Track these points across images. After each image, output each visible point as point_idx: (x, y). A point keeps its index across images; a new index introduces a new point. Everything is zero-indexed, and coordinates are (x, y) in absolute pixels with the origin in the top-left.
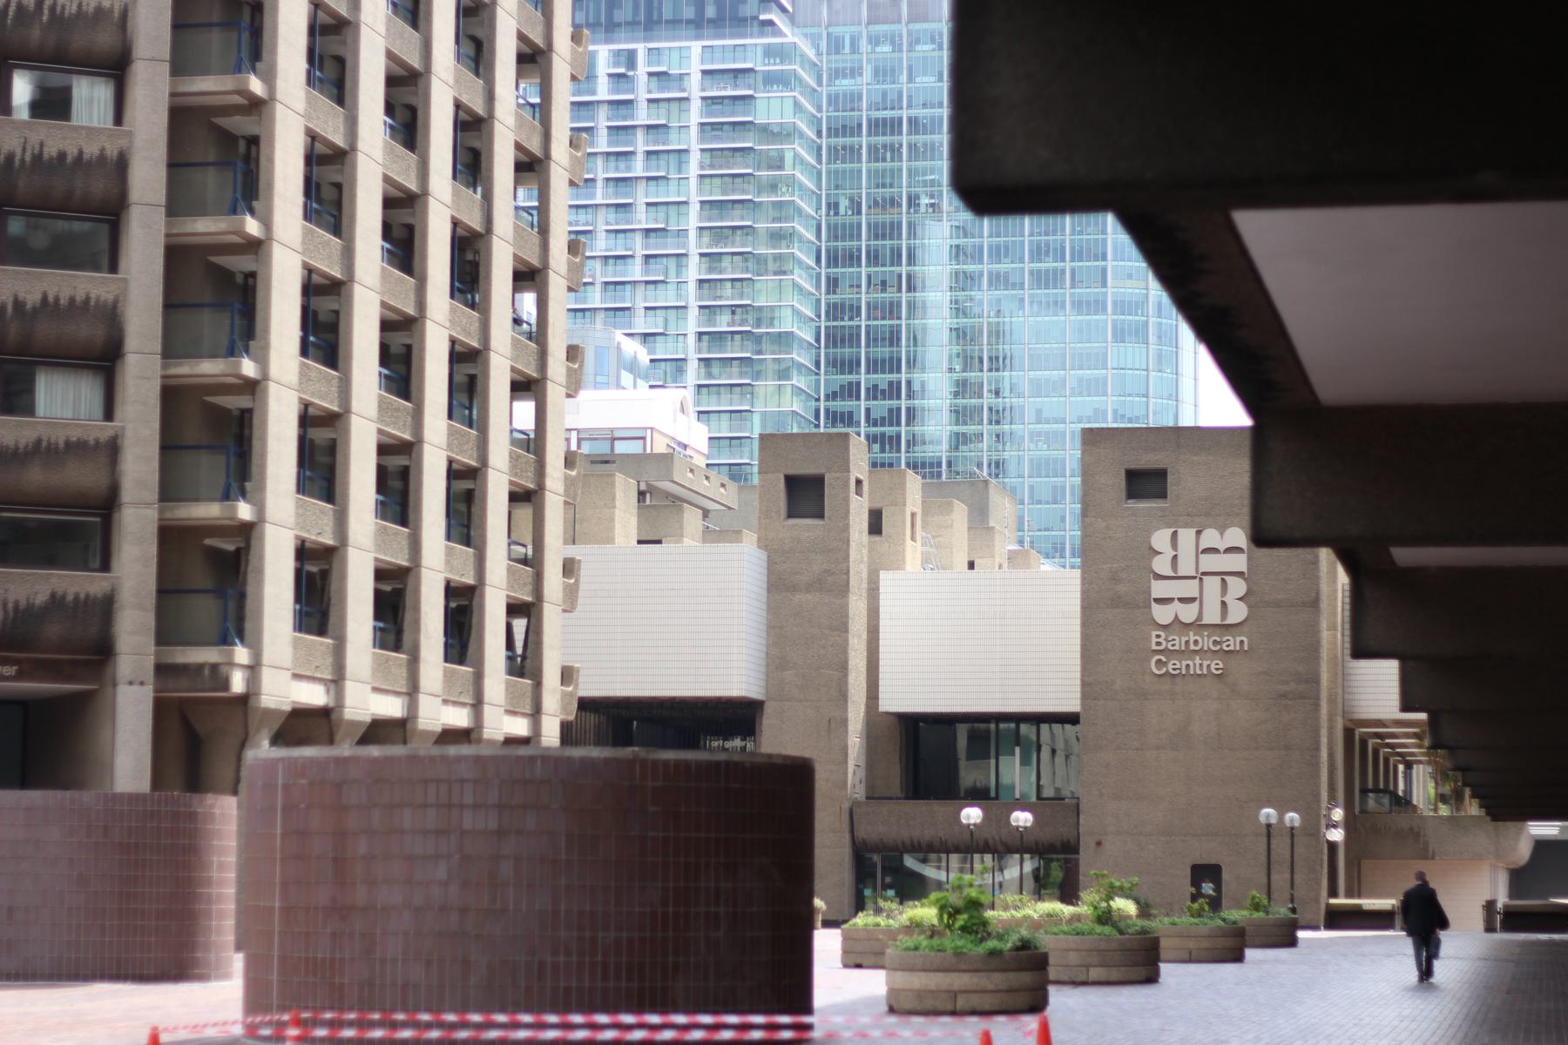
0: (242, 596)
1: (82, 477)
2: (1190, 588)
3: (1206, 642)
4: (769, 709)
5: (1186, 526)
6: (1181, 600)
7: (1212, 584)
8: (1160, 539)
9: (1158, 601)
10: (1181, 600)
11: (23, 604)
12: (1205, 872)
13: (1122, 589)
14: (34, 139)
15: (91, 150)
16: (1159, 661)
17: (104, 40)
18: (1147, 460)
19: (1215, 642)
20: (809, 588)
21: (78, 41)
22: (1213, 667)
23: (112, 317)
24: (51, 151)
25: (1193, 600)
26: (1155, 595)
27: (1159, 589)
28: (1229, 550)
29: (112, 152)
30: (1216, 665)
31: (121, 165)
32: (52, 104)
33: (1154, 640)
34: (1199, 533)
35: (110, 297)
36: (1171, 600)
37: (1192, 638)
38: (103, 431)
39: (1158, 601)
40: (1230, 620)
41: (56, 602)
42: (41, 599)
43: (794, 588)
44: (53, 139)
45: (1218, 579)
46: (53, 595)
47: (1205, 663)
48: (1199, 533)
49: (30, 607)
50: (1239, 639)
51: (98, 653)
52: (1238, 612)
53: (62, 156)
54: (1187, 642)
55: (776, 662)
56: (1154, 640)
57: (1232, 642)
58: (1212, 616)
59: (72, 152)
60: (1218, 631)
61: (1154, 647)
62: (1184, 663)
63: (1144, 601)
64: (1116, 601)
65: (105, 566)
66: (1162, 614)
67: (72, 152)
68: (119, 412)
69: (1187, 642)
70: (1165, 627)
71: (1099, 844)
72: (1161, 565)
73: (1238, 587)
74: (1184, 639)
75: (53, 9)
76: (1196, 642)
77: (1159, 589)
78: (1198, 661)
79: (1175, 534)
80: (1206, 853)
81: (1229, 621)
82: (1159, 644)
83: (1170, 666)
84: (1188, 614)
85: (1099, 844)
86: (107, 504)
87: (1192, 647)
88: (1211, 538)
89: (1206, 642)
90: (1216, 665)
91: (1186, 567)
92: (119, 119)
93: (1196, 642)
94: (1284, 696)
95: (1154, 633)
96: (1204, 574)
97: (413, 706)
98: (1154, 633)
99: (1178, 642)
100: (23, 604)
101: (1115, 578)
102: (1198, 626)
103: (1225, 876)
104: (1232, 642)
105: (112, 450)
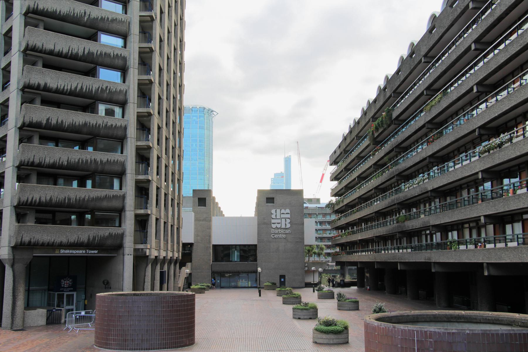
0: (147, 232)
1: (116, 204)
2: (279, 221)
3: (282, 231)
4: (194, 245)
7: (283, 220)
8: (273, 211)
11: (102, 236)
12: (282, 276)
13: (265, 221)
14: (105, 121)
15: (119, 124)
17: (121, 98)
18: (270, 196)
20: (203, 220)
21: (115, 97)
23: (123, 165)
24: (109, 124)
27: (273, 221)
29: (123, 125)
30: (284, 236)
31: (125, 128)
32: (110, 113)
35: (123, 160)
38: (121, 193)
41: (110, 235)
42: (107, 234)
43: (200, 220)
44: (110, 121)
46: (109, 233)
49: (104, 236)
51: (119, 247)
52: (288, 226)
53: (112, 125)
55: (196, 235)
57: (287, 231)
58: (283, 226)
59: (114, 125)
63: (271, 223)
64: (264, 223)
65: (120, 226)
66: (274, 226)
67: (114, 125)
68: (124, 188)
72: (273, 216)
73: (288, 221)
75: (109, 89)
77: (273, 221)
80: (282, 273)
84: (279, 226)
86: (121, 211)
88: (283, 211)
89: (282, 231)
90: (284, 236)
91: (278, 217)
92: (123, 117)
94: (297, 242)
97: (159, 253)
99: (277, 231)
100: (102, 236)
101: (264, 219)
102: (281, 228)
103: (286, 277)
104: (287, 231)
105: (124, 197)
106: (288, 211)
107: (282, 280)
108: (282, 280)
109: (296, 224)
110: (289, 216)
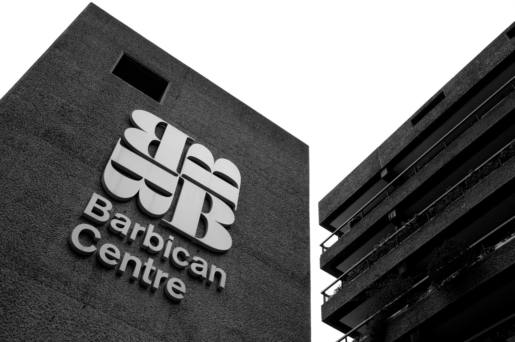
3: (170, 248)
10: (149, 184)
13: (68, 129)
19: (181, 256)
22: (170, 285)
33: (92, 203)
40: (207, 240)
47: (160, 274)
48: (189, 143)
52: (218, 239)
54: (141, 234)
56: (92, 203)
57: (203, 267)
61: (88, 211)
70: (116, 200)
76: (154, 241)
83: (103, 250)
87: (147, 242)
89: (170, 248)
93: (154, 241)
95: (96, 197)
98: (96, 197)
99: (128, 226)
109: (266, 261)
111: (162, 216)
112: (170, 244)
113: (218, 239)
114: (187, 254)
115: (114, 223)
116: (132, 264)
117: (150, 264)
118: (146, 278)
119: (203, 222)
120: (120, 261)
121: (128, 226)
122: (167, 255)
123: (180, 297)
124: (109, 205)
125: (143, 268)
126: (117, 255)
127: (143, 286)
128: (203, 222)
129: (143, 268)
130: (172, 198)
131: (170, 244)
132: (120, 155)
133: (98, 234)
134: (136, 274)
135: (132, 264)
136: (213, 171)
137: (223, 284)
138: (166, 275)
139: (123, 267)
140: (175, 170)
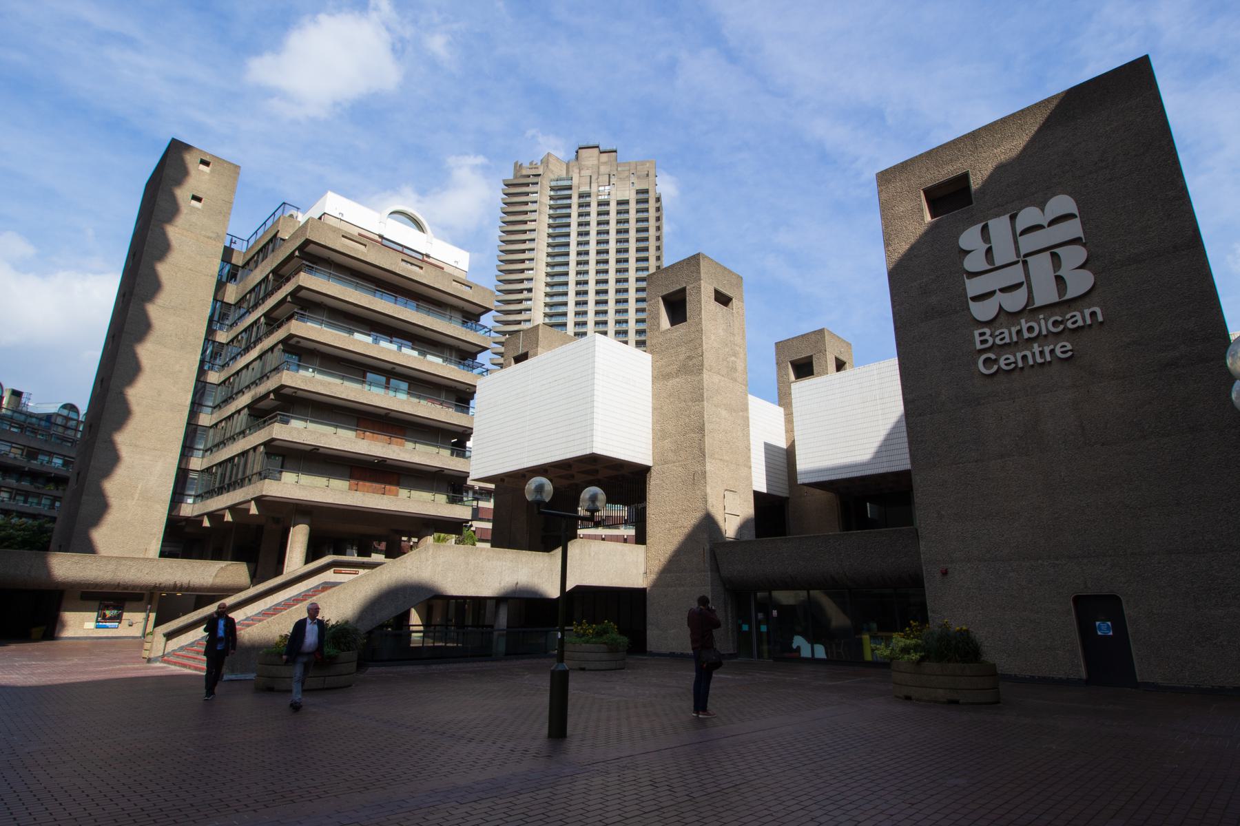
3: (1044, 325)
4: (653, 472)
5: (997, 215)
6: (1002, 290)
8: (970, 238)
9: (975, 299)
10: (1002, 290)
16: (986, 361)
19: (1055, 323)
22: (1058, 351)
25: (1019, 285)
26: (970, 294)
28: (1053, 222)
33: (978, 339)
34: (1013, 218)
36: (992, 293)
37: (1025, 326)
39: (975, 299)
45: (1047, 254)
47: (1047, 350)
48: (1013, 218)
50: (1087, 312)
52: (1080, 282)
54: (1019, 332)
56: (978, 339)
57: (1079, 318)
58: (1046, 294)
60: (1057, 310)
61: (979, 346)
62: (1019, 355)
63: (962, 303)
66: (983, 311)
69: (1019, 332)
71: (945, 573)
72: (974, 262)
74: (1014, 330)
78: (1036, 348)
79: (985, 229)
81: (1068, 296)
82: (985, 341)
83: (1002, 363)
85: (945, 573)
87: (1026, 335)
88: (1029, 216)
89: (1044, 325)
90: (1062, 348)
93: (1030, 329)
95: (976, 333)
96: (1026, 256)
99: (1007, 334)
102: (1029, 310)
103: (1128, 611)
104: (1079, 318)
106: (1063, 203)
107: (1104, 628)
108: (1104, 628)
110: (1074, 229)
111: (1027, 305)
112: (1043, 322)
113: (1080, 282)
114: (1060, 319)
115: (998, 342)
116: (1024, 358)
117: (1036, 348)
118: (1039, 360)
119: (1060, 280)
120: (1015, 363)
121: (1007, 334)
122: (1044, 332)
123: (1070, 354)
124: (987, 331)
125: (1033, 354)
126: (1012, 359)
127: (1042, 364)
128: (1060, 280)
129: (1033, 354)
130: (1025, 285)
131: (1043, 322)
132: (974, 287)
133: (993, 356)
134: (1031, 362)
135: (1024, 358)
136: (1045, 224)
137: (1100, 319)
138: (1052, 347)
139: (1020, 364)
140: (1016, 259)
